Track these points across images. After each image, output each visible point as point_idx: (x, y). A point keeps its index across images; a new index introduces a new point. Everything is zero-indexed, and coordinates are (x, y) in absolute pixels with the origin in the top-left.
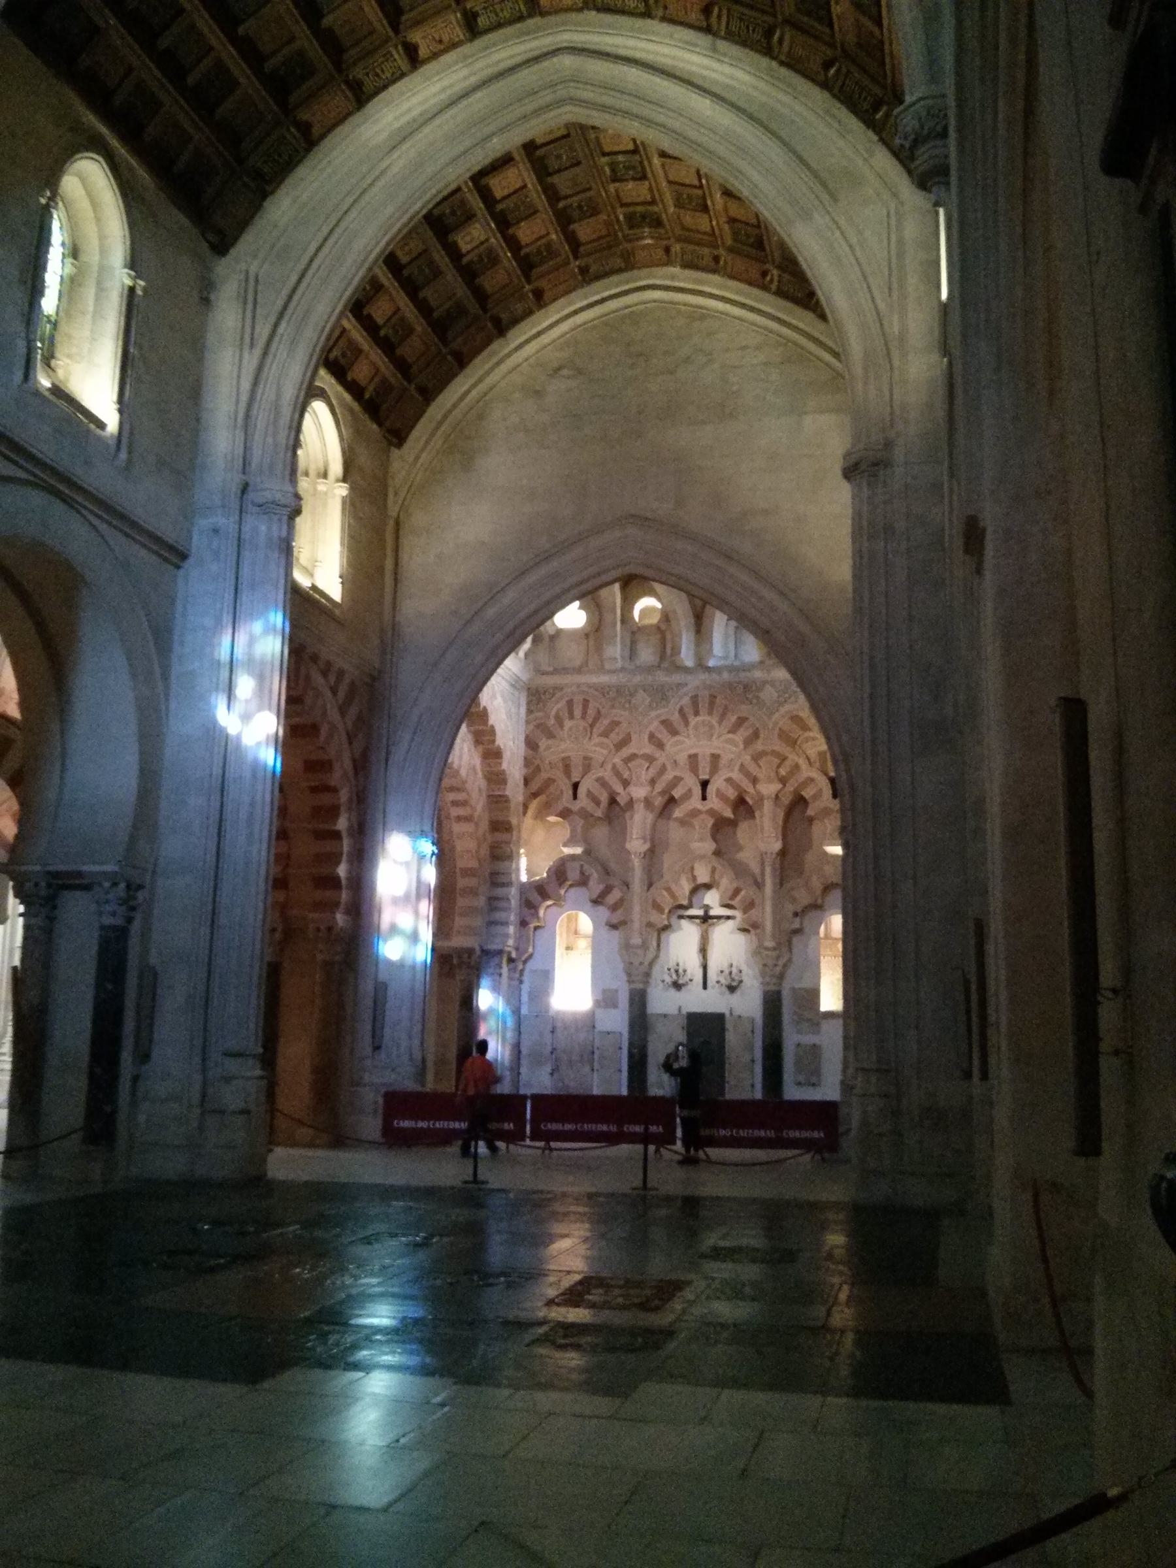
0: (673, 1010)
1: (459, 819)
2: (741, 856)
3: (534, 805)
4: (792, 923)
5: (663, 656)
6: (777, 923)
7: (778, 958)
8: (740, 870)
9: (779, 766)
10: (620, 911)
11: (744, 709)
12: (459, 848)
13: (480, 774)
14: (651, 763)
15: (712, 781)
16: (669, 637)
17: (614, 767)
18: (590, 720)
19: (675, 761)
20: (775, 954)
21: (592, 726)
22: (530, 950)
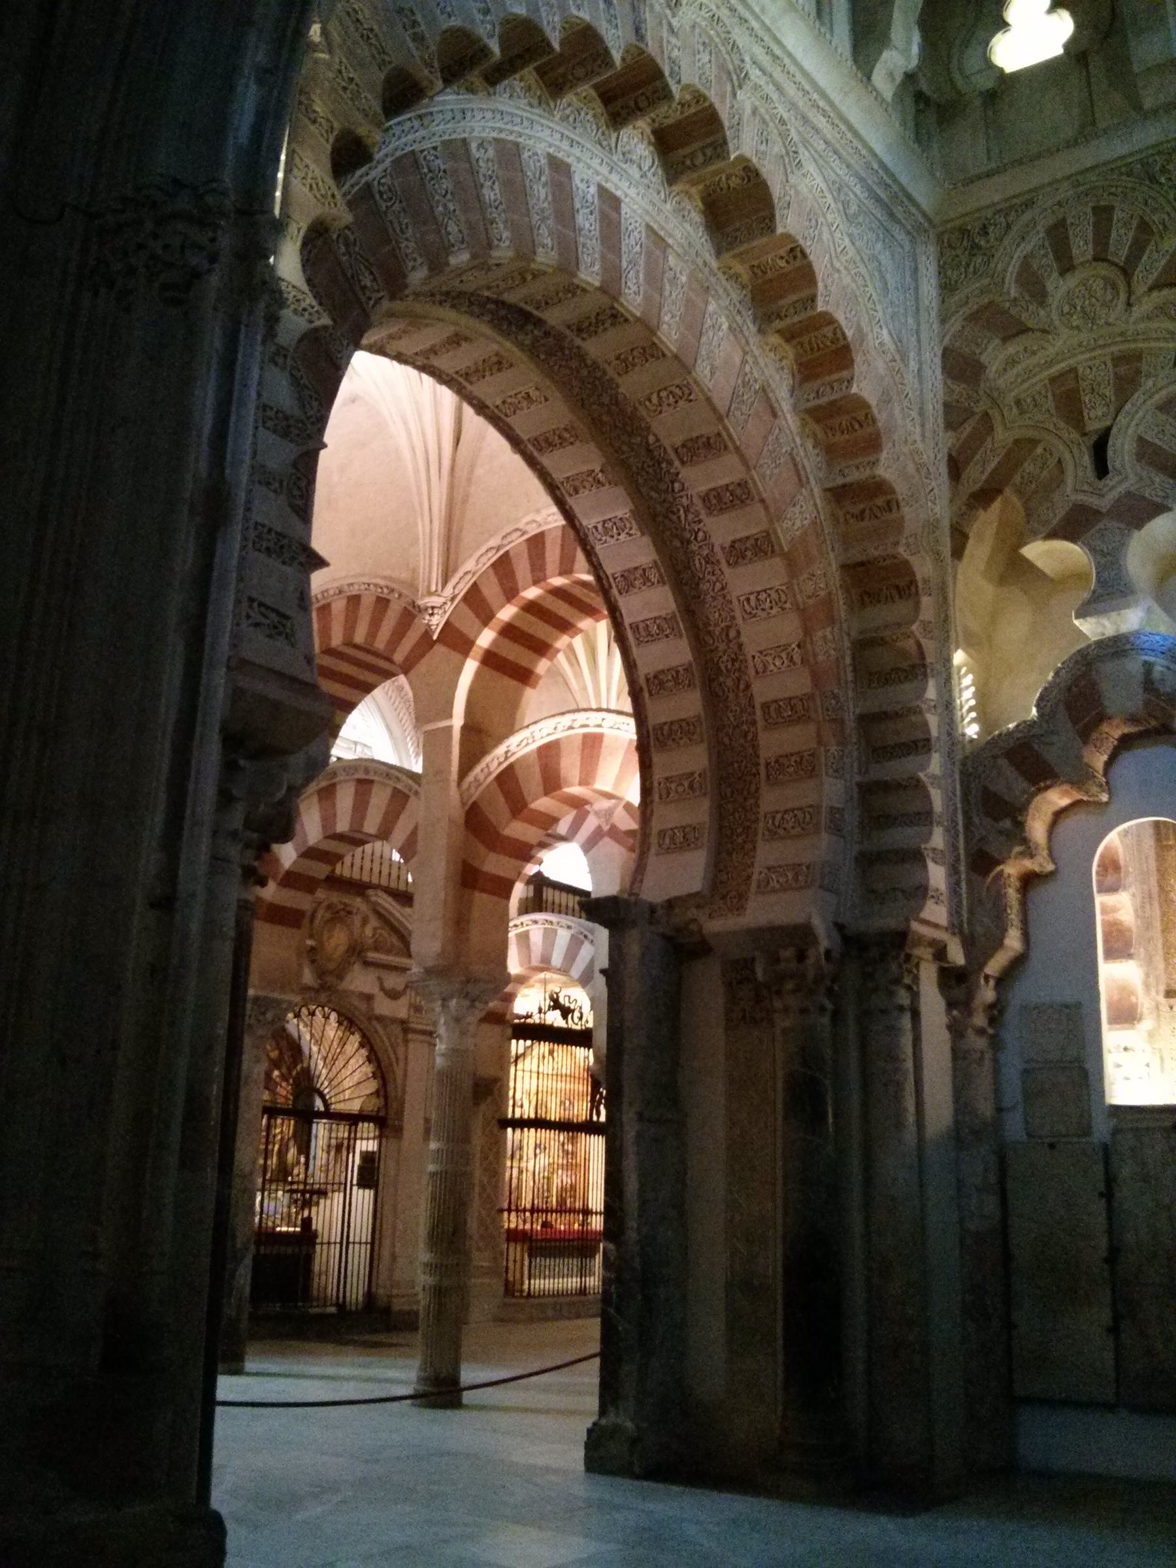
1: (738, 552)
12: (750, 650)
13: (790, 420)
18: (1124, 252)
21: (1127, 272)
22: (1013, 941)
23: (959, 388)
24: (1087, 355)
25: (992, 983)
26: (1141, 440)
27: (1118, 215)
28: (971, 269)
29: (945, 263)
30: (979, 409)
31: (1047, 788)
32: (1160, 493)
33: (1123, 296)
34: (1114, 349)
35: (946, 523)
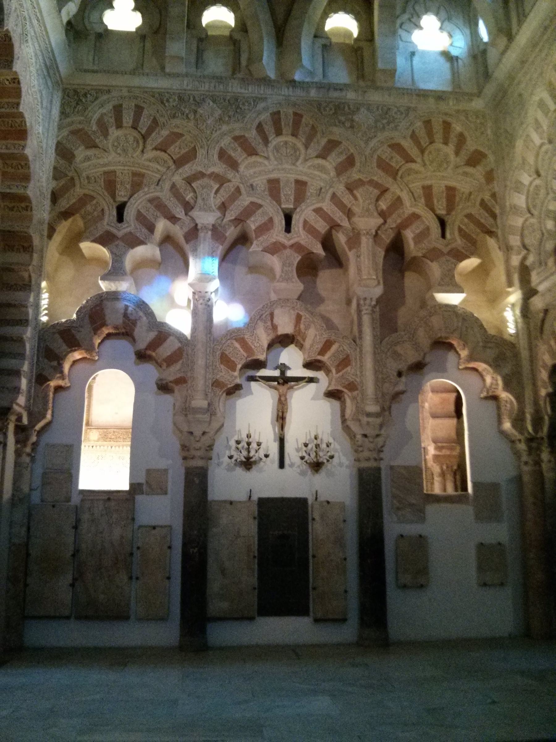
0: (241, 496)
2: (322, 308)
3: (63, 228)
4: (396, 384)
5: (236, 67)
6: (379, 381)
7: (381, 426)
8: (329, 324)
9: (377, 200)
10: (177, 366)
11: (337, 132)
14: (221, 185)
15: (298, 210)
16: (244, 47)
17: (173, 186)
19: (252, 185)
20: (379, 420)
21: (144, 138)
22: (49, 416)
23: (62, 162)
24: (122, 168)
25: (36, 432)
26: (139, 211)
27: (145, 112)
28: (76, 110)
29: (65, 102)
30: (70, 174)
31: (75, 350)
32: (144, 237)
33: (141, 148)
34: (133, 169)
35: (46, 222)
